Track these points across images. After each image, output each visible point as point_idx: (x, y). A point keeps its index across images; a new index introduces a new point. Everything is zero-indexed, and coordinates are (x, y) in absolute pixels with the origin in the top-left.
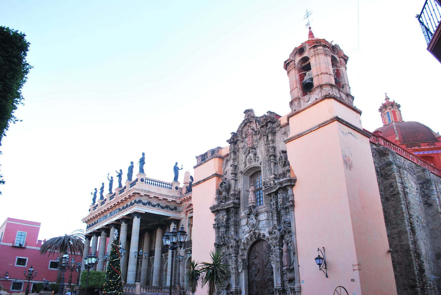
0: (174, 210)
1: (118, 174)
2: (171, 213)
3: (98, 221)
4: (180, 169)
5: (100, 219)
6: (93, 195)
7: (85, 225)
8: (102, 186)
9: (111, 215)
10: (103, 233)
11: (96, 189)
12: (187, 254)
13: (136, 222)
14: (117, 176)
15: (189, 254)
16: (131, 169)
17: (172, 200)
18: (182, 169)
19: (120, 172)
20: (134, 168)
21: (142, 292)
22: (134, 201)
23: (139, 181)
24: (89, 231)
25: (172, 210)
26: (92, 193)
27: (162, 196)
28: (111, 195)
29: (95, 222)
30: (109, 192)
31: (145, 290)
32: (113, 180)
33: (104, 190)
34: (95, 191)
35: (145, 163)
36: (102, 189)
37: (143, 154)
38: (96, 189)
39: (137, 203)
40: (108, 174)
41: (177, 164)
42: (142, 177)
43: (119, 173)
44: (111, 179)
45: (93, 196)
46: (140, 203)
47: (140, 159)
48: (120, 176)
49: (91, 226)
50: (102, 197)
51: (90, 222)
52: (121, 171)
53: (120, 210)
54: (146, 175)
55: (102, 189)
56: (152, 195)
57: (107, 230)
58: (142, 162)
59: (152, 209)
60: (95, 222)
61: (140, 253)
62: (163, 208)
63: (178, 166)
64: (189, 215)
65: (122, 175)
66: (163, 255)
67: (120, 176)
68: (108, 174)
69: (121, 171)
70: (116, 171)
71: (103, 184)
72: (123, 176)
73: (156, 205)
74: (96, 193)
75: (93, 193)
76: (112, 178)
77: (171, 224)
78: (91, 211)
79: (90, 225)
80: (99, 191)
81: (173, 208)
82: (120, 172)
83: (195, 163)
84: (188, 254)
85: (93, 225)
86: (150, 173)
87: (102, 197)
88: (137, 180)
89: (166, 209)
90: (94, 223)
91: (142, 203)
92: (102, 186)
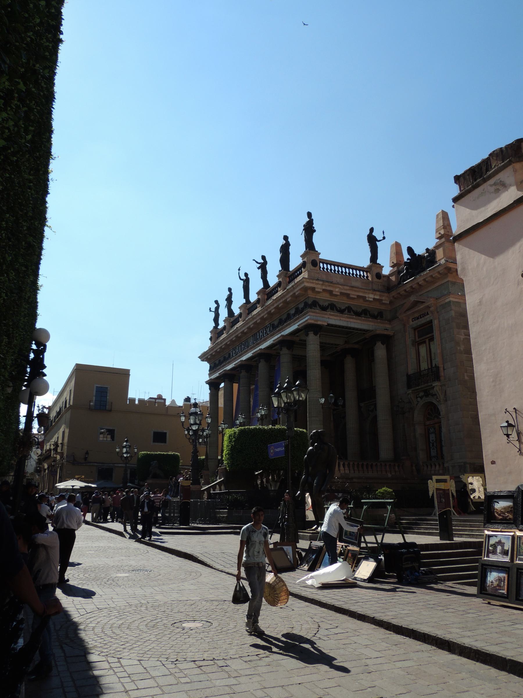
0: (379, 318)
1: (259, 265)
2: (373, 324)
3: (230, 354)
5: (234, 349)
7: (206, 366)
8: (229, 293)
9: (256, 340)
10: (243, 374)
11: (216, 302)
12: (417, 398)
13: (313, 343)
14: (259, 268)
15: (421, 398)
16: (285, 250)
17: (374, 299)
18: (384, 238)
19: (262, 261)
20: (290, 247)
21: (342, 472)
22: (303, 304)
23: (309, 265)
24: (216, 375)
25: (374, 317)
26: (210, 308)
27: (355, 291)
28: (249, 306)
29: (225, 357)
30: (244, 301)
31: (347, 468)
32: (249, 278)
33: (233, 299)
34: (216, 305)
35: (315, 231)
36: (229, 300)
37: (309, 215)
38: (216, 302)
39: (311, 308)
40: (239, 270)
41: (372, 230)
42: (313, 258)
43: (259, 263)
45: (213, 315)
46: (315, 306)
47: (304, 226)
48: (263, 267)
49: (218, 366)
50: (231, 312)
51: (214, 358)
52: (263, 258)
54: (319, 254)
55: (229, 300)
56: (337, 290)
57: (248, 367)
58: (309, 229)
59: (338, 318)
60: (225, 357)
61: (329, 398)
62: (358, 314)
63: (374, 234)
65: (267, 266)
66: (362, 404)
67: (263, 267)
68: (239, 270)
69: (263, 258)
70: (254, 260)
71: (230, 290)
72: (268, 267)
73: (344, 310)
74: (217, 309)
76: (246, 275)
77: (375, 344)
78: (213, 340)
79: (215, 363)
80: (223, 304)
81: (376, 314)
82: (262, 261)
83: (455, 190)
84: (419, 399)
85: (220, 363)
86: (327, 249)
87: (231, 312)
88: (304, 265)
89: (363, 315)
90: (222, 359)
91: (320, 306)
92: (229, 293)
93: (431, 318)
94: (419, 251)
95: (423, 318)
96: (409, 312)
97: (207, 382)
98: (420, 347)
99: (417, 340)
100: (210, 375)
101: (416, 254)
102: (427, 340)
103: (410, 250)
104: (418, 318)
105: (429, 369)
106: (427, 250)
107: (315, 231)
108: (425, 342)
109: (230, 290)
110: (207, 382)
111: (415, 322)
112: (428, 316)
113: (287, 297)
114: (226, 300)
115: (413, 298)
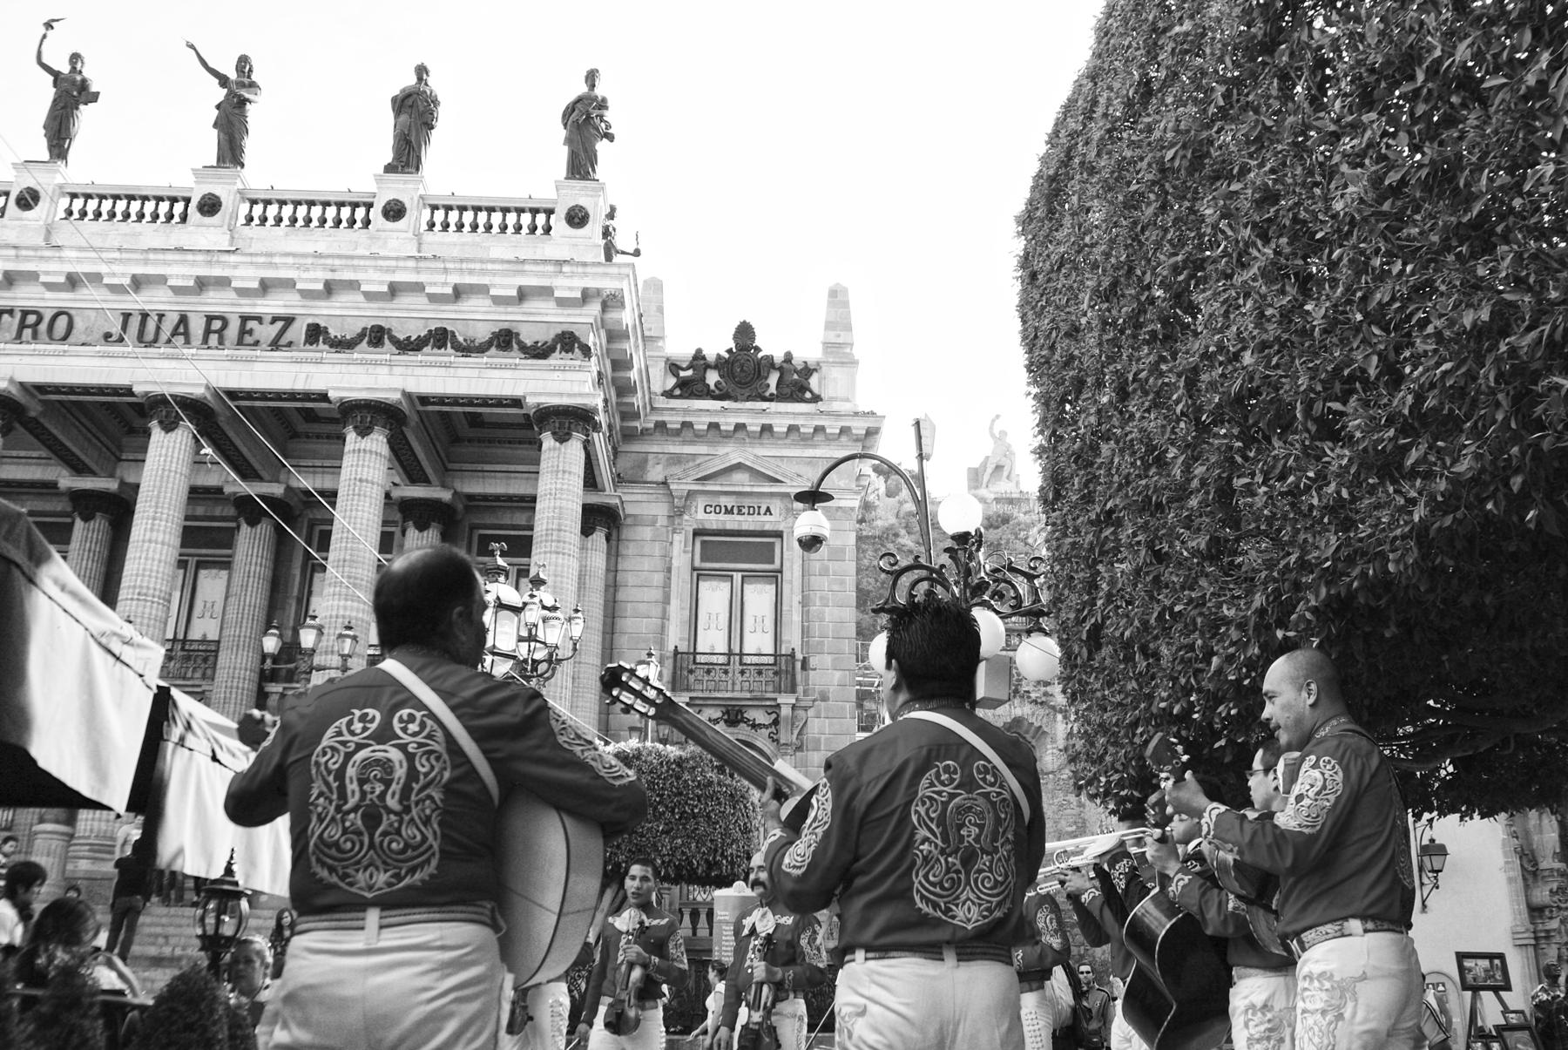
18: (637, 253)
40: (49, 25)
44: (65, 68)
53: (315, 333)
64: (701, 515)
68: (49, 25)
70: (192, 47)
94: (770, 345)
95: (750, 518)
98: (705, 586)
99: (697, 563)
101: (758, 349)
102: (738, 577)
103: (745, 332)
104: (729, 511)
107: (610, 137)
108: (726, 576)
112: (768, 518)
113: (497, 280)
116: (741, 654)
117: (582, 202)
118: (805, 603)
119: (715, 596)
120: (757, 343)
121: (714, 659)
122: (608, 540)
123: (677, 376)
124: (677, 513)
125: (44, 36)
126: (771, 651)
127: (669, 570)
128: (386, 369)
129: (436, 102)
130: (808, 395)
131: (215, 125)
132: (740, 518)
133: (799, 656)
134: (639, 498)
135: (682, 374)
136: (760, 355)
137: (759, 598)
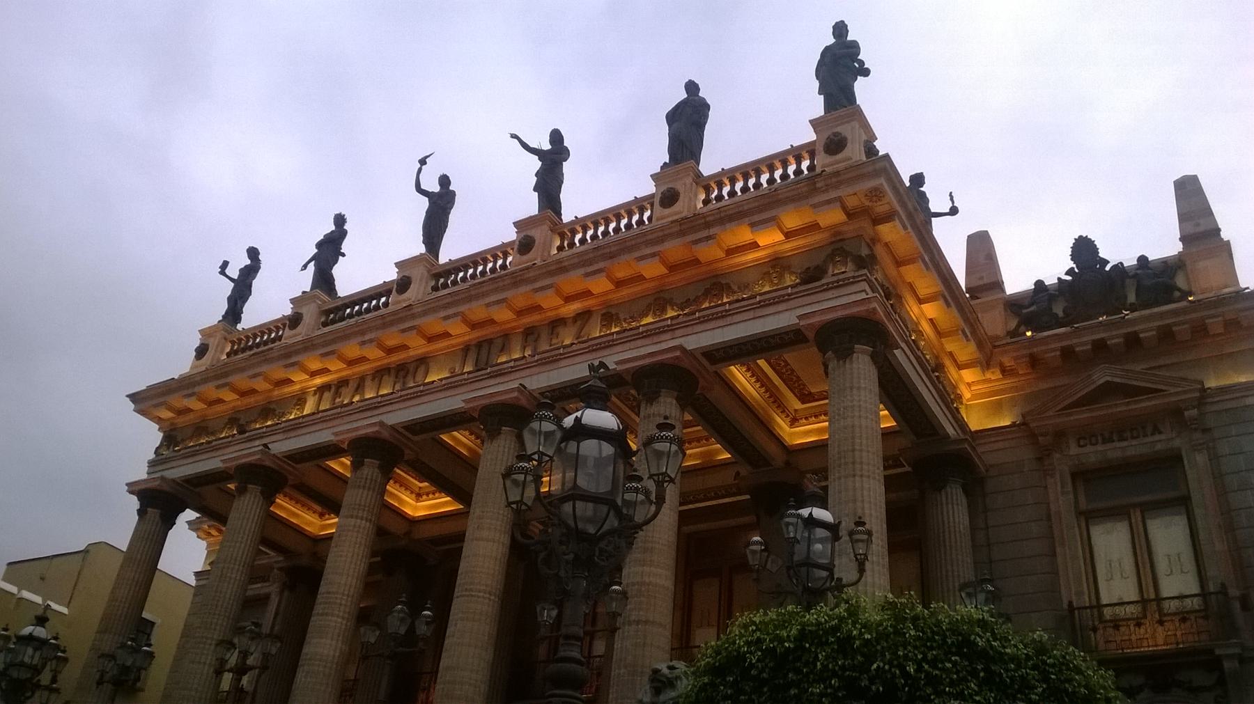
4: (934, 207)
6: (231, 285)
11: (253, 253)
18: (954, 211)
19: (547, 146)
33: (345, 248)
34: (248, 262)
38: (253, 253)
40: (423, 162)
44: (436, 188)
52: (556, 137)
55: (330, 249)
58: (840, 66)
64: (1074, 450)
65: (566, 166)
68: (423, 162)
69: (556, 137)
70: (514, 136)
71: (340, 220)
75: (234, 272)
76: (444, 181)
78: (207, 360)
93: (1177, 443)
95: (1134, 442)
96: (1082, 415)
97: (133, 488)
99: (1083, 505)
100: (152, 464)
105: (1143, 602)
106: (1142, 260)
107: (866, 73)
109: (340, 220)
110: (133, 488)
111: (1089, 449)
112: (1157, 437)
114: (319, 245)
115: (1101, 376)
116: (1159, 600)
117: (838, 129)
118: (1229, 527)
119: (1112, 542)
120: (1103, 254)
121: (1120, 611)
122: (966, 492)
123: (1017, 314)
124: (1043, 456)
125: (420, 170)
126: (1195, 589)
127: (1049, 518)
128: (668, 336)
129: (708, 107)
130: (1177, 294)
131: (535, 190)
132: (1125, 444)
133: (1234, 592)
134: (996, 446)
135: (1025, 311)
136: (1108, 268)
137: (1168, 536)
